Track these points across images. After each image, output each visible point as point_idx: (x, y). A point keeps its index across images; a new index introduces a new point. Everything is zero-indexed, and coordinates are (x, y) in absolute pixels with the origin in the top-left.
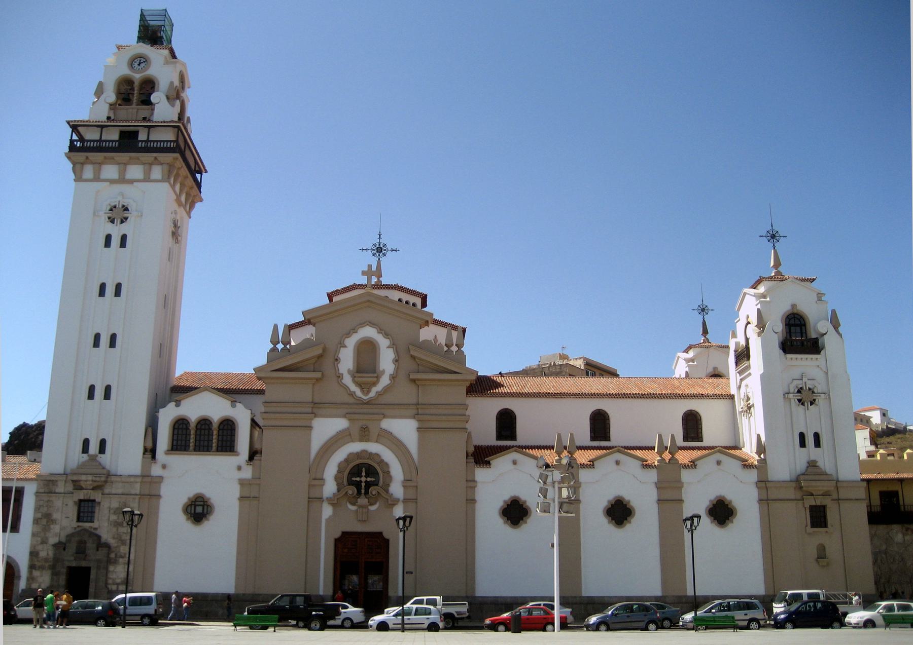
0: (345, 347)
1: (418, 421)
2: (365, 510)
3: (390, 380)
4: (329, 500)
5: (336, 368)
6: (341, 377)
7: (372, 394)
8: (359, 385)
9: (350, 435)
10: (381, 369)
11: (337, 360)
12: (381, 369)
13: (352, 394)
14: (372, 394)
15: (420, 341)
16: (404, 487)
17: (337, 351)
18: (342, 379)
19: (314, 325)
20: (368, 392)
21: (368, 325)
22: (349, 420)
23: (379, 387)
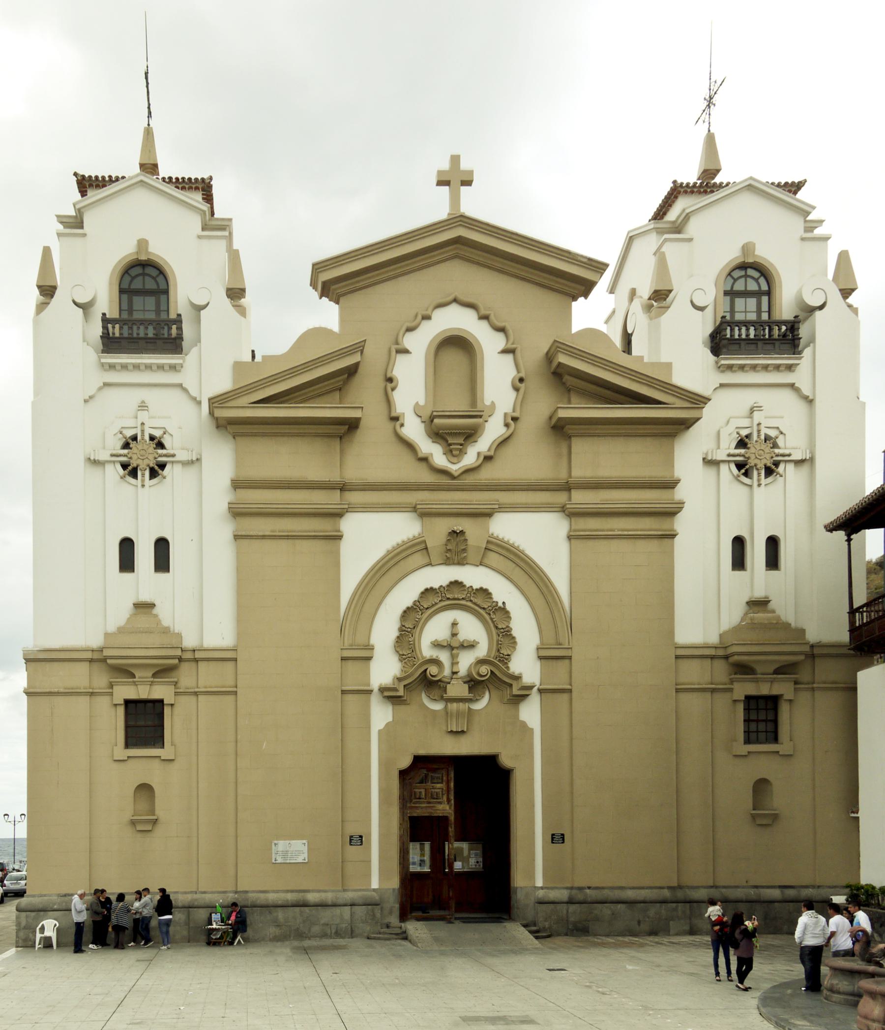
0: (406, 351)
1: (572, 514)
2: (463, 706)
3: (507, 425)
4: (382, 690)
5: (389, 402)
6: (401, 419)
7: (470, 458)
8: (437, 435)
9: (426, 548)
10: (488, 403)
11: (390, 380)
12: (488, 403)
13: (425, 460)
14: (470, 458)
15: (573, 332)
16: (541, 658)
17: (389, 363)
18: (402, 425)
19: (337, 302)
20: (462, 452)
21: (455, 300)
22: (424, 514)
23: (483, 444)
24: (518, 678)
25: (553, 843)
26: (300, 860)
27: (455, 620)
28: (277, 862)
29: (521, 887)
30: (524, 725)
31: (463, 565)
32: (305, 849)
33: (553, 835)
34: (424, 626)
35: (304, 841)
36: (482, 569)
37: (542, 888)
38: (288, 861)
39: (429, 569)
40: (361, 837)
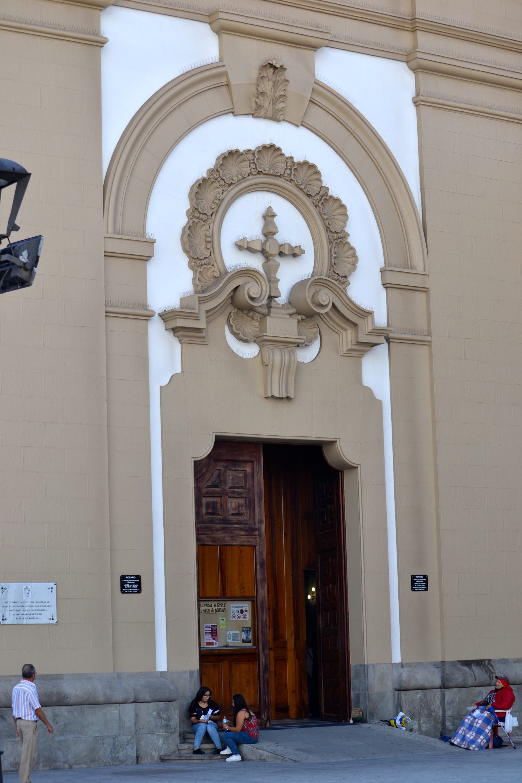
16: (386, 286)
24: (366, 314)
25: (413, 590)
26: (44, 619)
27: (270, 208)
28: (6, 622)
29: (373, 665)
30: (368, 391)
31: (278, 121)
32: (52, 598)
33: (413, 577)
34: (224, 216)
35: (52, 585)
36: (303, 132)
37: (402, 665)
38: (25, 622)
39: (229, 120)
40: (138, 577)
